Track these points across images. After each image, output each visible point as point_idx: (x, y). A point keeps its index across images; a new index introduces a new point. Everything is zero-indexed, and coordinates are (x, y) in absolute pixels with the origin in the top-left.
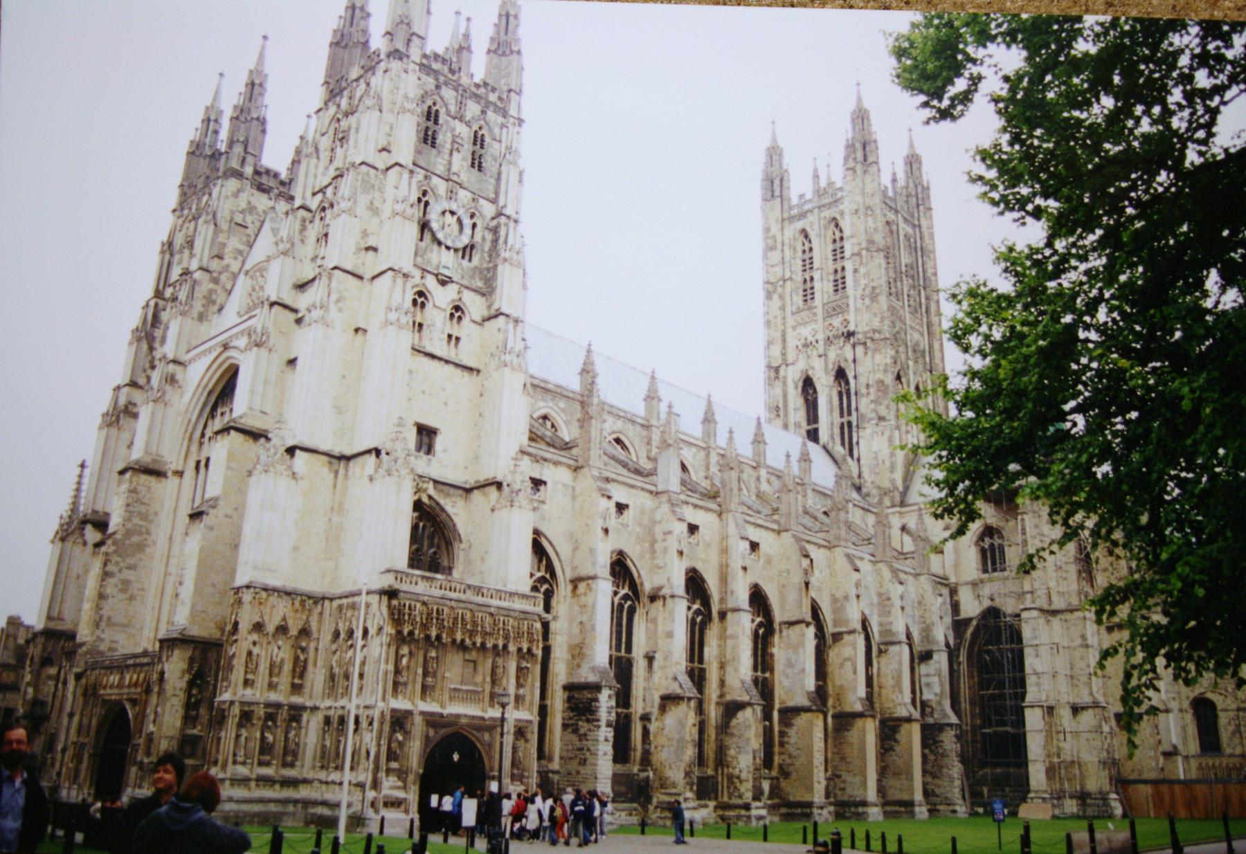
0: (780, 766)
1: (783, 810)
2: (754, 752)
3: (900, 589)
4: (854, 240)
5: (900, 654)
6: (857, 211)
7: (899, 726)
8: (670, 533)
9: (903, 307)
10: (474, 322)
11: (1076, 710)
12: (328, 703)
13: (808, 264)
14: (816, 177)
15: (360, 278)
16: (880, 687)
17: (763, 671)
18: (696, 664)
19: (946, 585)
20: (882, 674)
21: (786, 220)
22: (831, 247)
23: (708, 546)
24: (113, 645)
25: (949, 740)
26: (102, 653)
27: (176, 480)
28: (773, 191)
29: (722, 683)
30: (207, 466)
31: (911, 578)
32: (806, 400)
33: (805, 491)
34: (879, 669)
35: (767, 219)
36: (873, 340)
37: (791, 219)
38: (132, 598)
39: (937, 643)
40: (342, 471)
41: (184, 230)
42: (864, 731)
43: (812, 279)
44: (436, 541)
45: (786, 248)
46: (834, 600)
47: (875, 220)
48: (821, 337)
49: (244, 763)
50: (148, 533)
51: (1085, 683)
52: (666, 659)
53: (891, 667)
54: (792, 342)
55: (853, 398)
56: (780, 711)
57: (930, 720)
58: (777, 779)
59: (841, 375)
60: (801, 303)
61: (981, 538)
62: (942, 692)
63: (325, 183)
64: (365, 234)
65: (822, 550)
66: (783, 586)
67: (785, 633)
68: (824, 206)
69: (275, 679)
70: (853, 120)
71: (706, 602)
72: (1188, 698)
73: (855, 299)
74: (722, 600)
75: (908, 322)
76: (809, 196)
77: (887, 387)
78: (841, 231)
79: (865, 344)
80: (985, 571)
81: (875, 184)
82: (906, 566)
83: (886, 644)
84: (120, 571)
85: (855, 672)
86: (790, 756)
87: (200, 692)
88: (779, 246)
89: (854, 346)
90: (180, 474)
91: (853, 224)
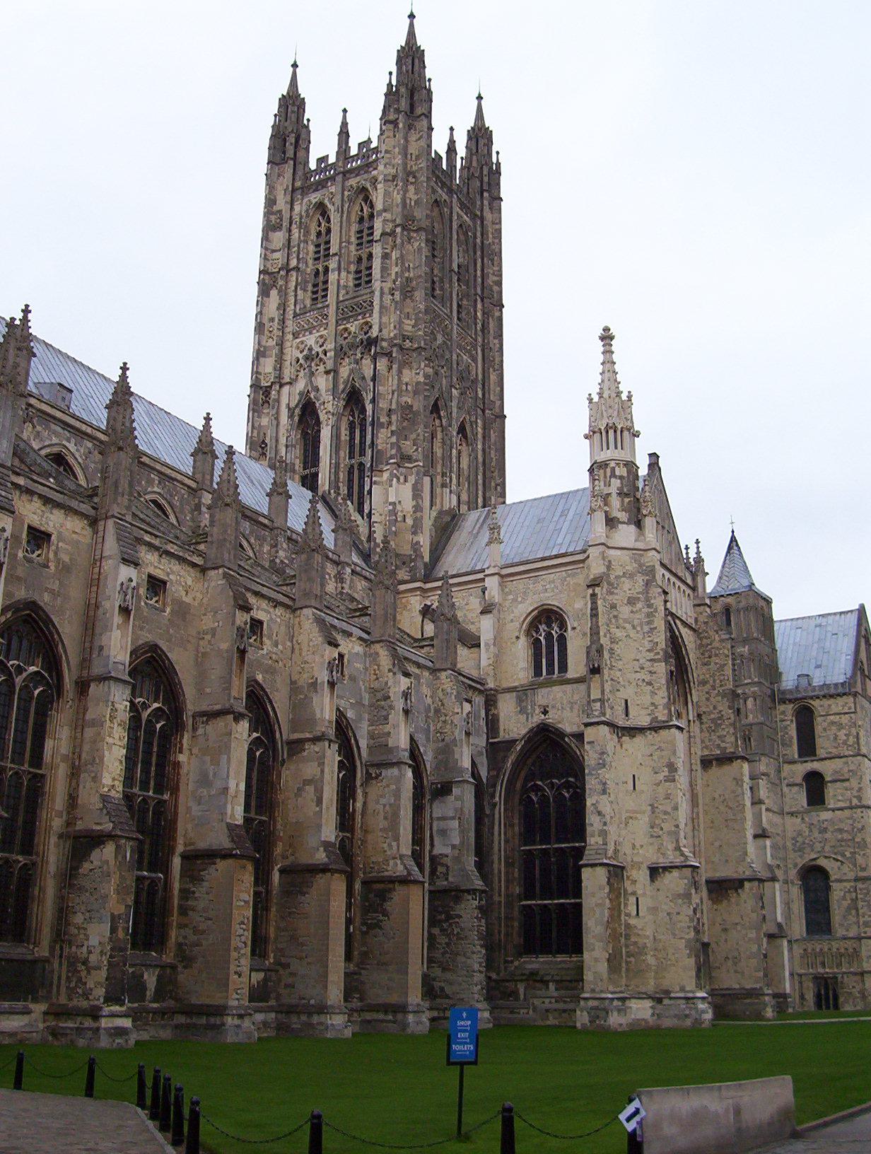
0: (180, 945)
1: (181, 1019)
2: (114, 919)
3: (404, 682)
4: (388, 216)
5: (399, 780)
6: (394, 177)
7: (390, 890)
9: (451, 319)
11: (654, 872)
13: (323, 252)
14: (344, 134)
16: (366, 831)
17: (159, 789)
18: (26, 767)
19: (480, 691)
20: (370, 811)
21: (294, 192)
22: (355, 227)
23: (65, 569)
25: (468, 911)
28: (284, 153)
29: (72, 800)
31: (426, 674)
32: (305, 435)
33: (275, 538)
34: (365, 803)
35: (271, 187)
36: (401, 348)
37: (305, 190)
39: (461, 771)
42: (327, 895)
43: (326, 269)
45: (294, 226)
46: (294, 687)
48: (330, 346)
51: (669, 833)
53: (383, 801)
54: (292, 353)
55: (369, 429)
56: (185, 857)
57: (442, 884)
58: (173, 967)
59: (353, 399)
60: (308, 302)
61: (533, 626)
62: (462, 843)
65: (279, 611)
66: (204, 654)
67: (200, 731)
68: (351, 171)
70: (399, 62)
71: (53, 664)
72: (796, 865)
73: (382, 294)
74: (85, 662)
75: (455, 335)
76: (332, 160)
77: (417, 414)
78: (372, 207)
79: (389, 355)
80: (538, 672)
81: (423, 143)
82: (420, 655)
83: (380, 765)
85: (319, 801)
86: (196, 931)
88: (285, 224)
91: (387, 194)
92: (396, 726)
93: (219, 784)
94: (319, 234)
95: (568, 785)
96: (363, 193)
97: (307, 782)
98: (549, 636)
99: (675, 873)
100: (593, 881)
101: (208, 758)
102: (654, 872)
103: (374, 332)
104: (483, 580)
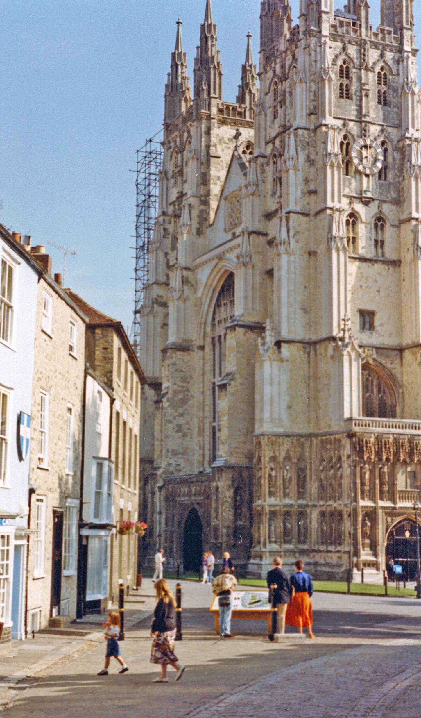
10: (393, 226)
12: (321, 503)
15: (307, 215)
24: (178, 468)
26: (172, 473)
27: (201, 353)
30: (220, 343)
38: (185, 435)
40: (312, 352)
41: (174, 160)
44: (382, 389)
49: (276, 542)
50: (188, 390)
63: (273, 135)
64: (307, 181)
69: (287, 490)
84: (175, 418)
87: (241, 498)
90: (202, 348)
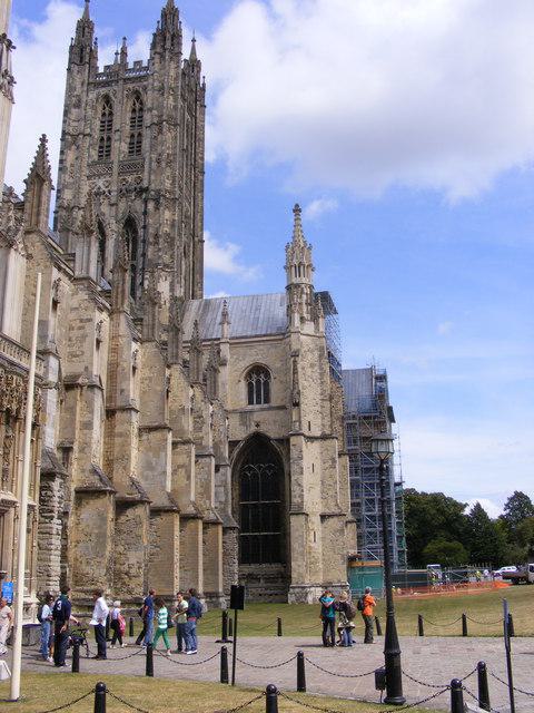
8: (90, 320)
13: (107, 124)
22: (129, 115)
28: (81, 58)
37: (98, 85)
43: (109, 139)
47: (175, 100)
52: (82, 450)
55: (141, 245)
59: (130, 224)
60: (96, 158)
61: (249, 375)
67: (144, 437)
78: (141, 103)
79: (157, 202)
80: (251, 402)
85: (189, 478)
89: (146, 202)
92: (207, 434)
93: (160, 469)
94: (104, 115)
95: (269, 468)
96: (138, 96)
97: (182, 466)
98: (258, 382)
99: (335, 519)
100: (295, 522)
101: (151, 454)
102: (323, 517)
103: (145, 184)
104: (218, 345)
